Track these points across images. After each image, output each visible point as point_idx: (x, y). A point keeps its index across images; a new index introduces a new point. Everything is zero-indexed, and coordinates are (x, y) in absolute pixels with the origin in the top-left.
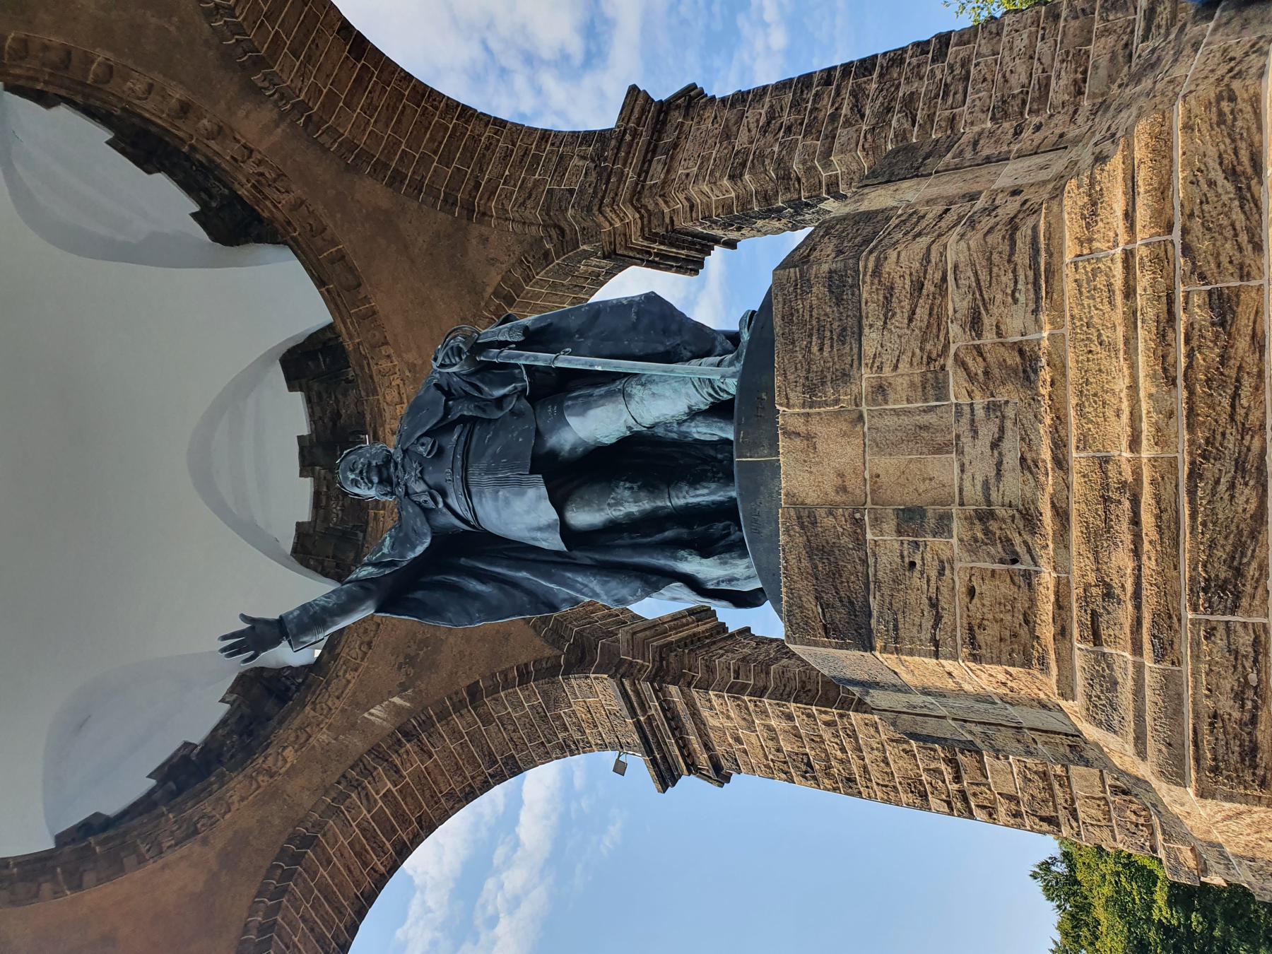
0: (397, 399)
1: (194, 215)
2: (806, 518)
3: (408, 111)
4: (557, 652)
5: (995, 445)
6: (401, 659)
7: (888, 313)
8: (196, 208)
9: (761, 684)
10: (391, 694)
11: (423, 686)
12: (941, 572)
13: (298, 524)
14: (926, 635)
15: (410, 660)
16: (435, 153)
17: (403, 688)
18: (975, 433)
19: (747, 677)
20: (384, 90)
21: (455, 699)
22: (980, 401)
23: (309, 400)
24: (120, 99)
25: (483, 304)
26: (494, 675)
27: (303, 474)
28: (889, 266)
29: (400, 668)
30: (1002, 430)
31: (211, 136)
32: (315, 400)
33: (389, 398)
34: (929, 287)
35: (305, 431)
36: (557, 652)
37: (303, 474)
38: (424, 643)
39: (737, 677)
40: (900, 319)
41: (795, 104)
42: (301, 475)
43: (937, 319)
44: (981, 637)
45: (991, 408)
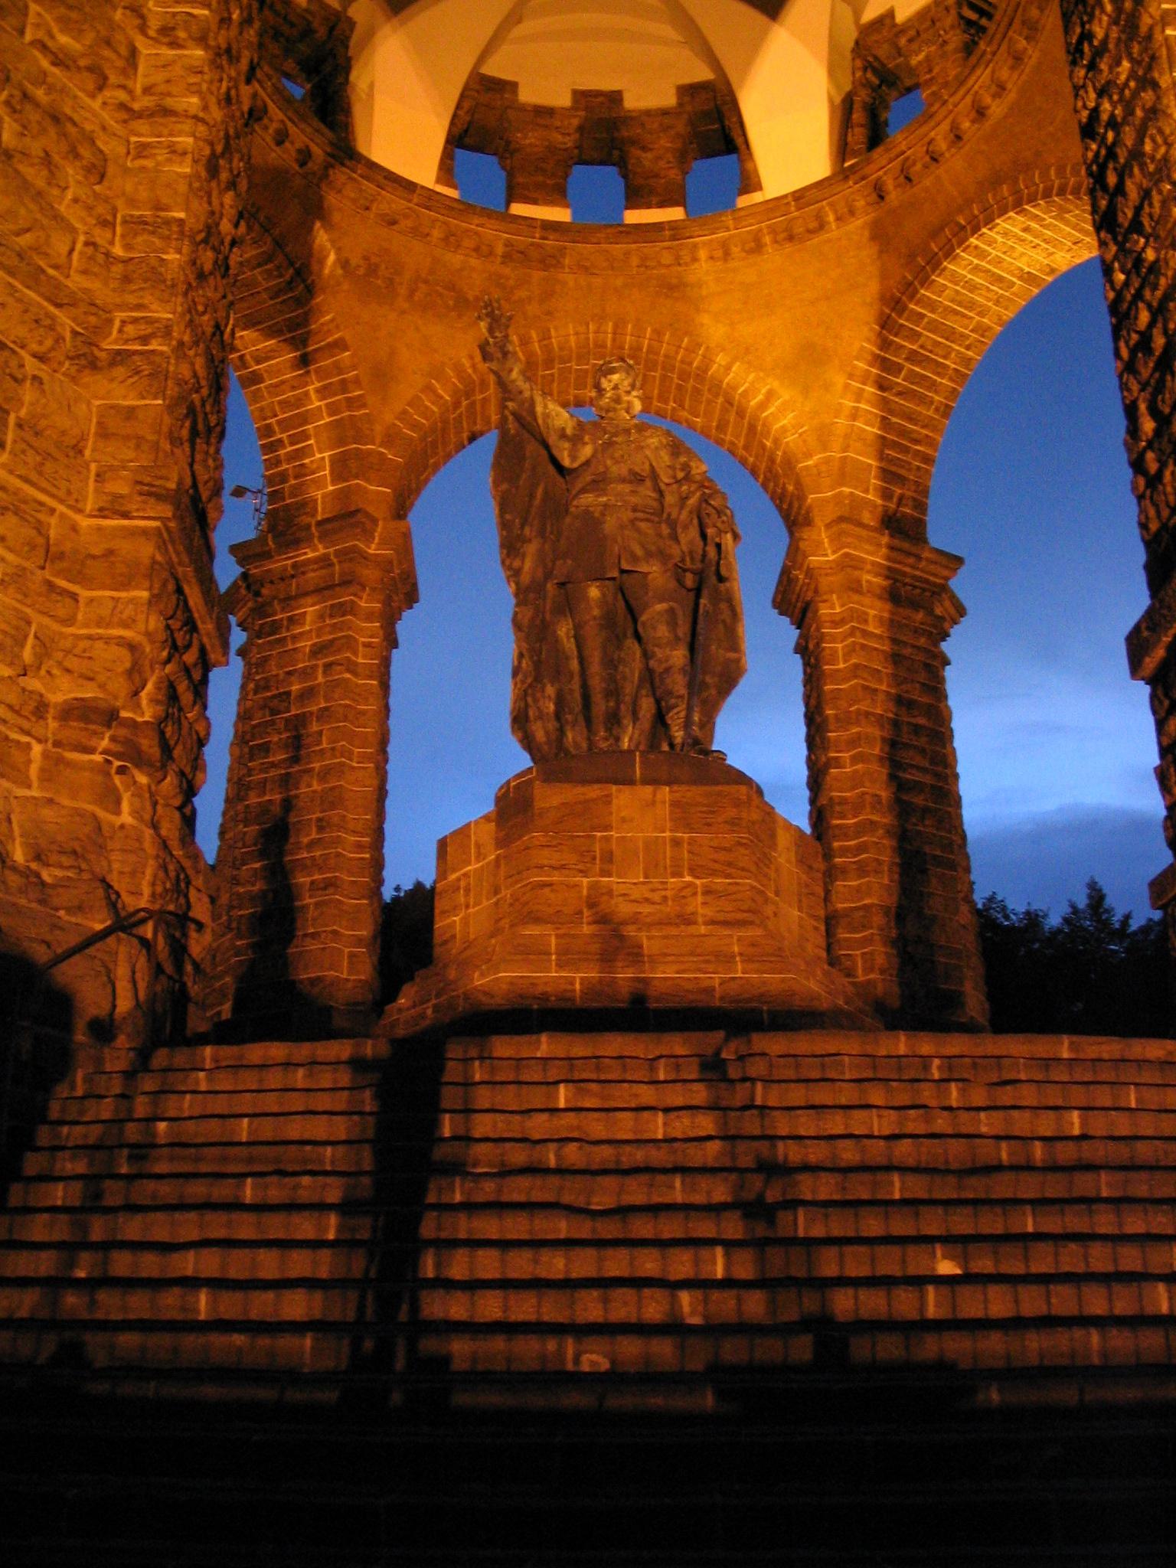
0: (663, 261)
1: (890, 14)
2: (607, 800)
3: (966, 321)
4: (378, 440)
5: (647, 900)
6: (374, 260)
7: (717, 849)
8: (901, 17)
9: (360, 670)
10: (339, 250)
11: (345, 287)
12: (581, 871)
13: (513, 86)
14: (546, 862)
15: (372, 270)
16: (922, 347)
17: (344, 264)
18: (653, 890)
19: (364, 657)
20: (989, 299)
21: (331, 326)
22: (669, 893)
23: (665, 112)
24: (994, 54)
25: (762, 374)
26: (354, 367)
27: (580, 96)
28: (742, 850)
29: (366, 258)
30: (653, 903)
31: (955, 128)
32: (667, 120)
33: (665, 253)
34: (730, 871)
35: (630, 103)
36: (378, 440)
37: (580, 96)
38: (390, 283)
39: (365, 645)
40: (715, 856)
41: (917, 729)
42: (575, 92)
43: (713, 873)
44: (547, 890)
45: (665, 898)
